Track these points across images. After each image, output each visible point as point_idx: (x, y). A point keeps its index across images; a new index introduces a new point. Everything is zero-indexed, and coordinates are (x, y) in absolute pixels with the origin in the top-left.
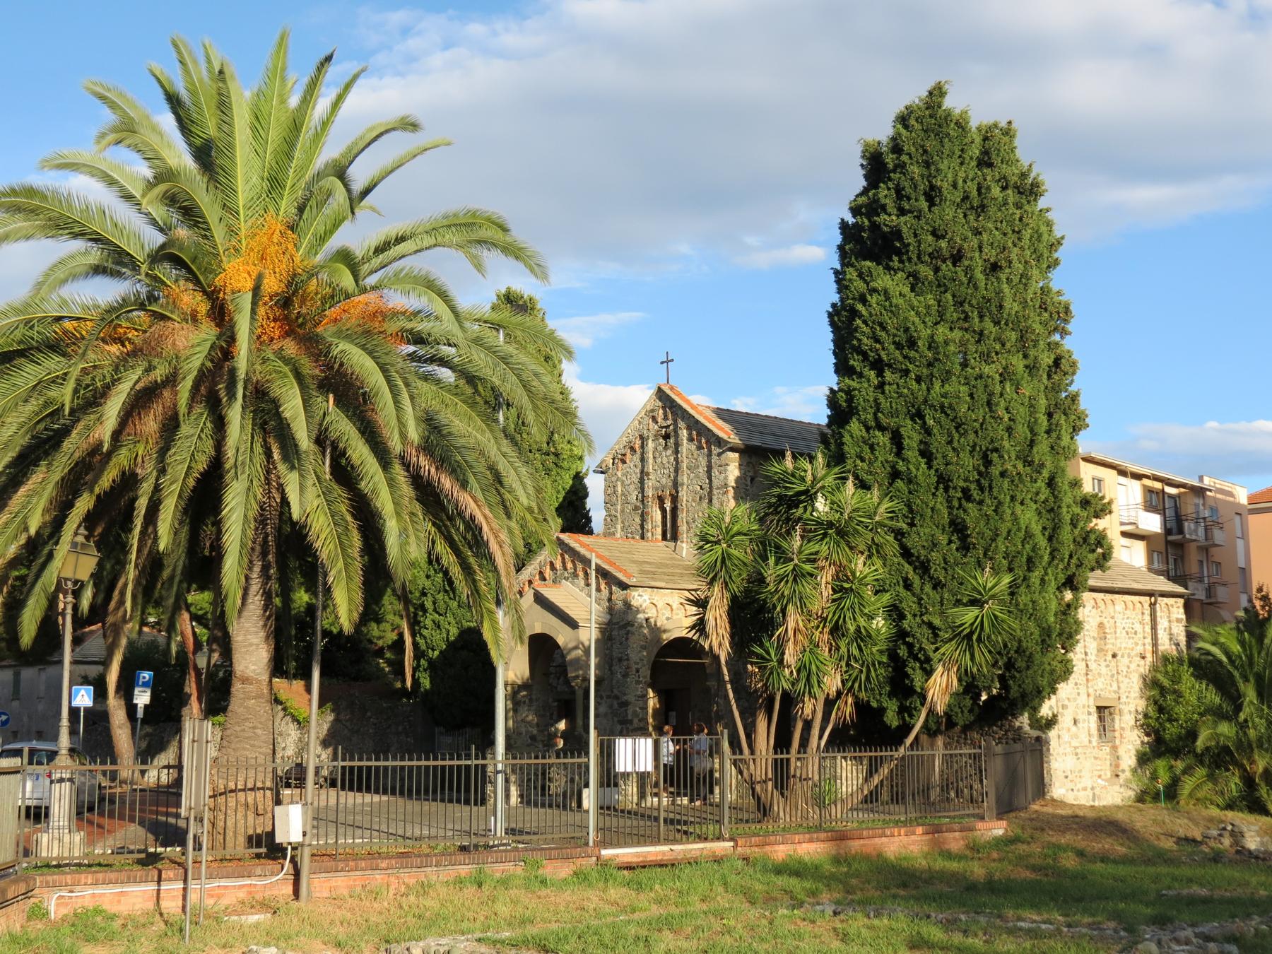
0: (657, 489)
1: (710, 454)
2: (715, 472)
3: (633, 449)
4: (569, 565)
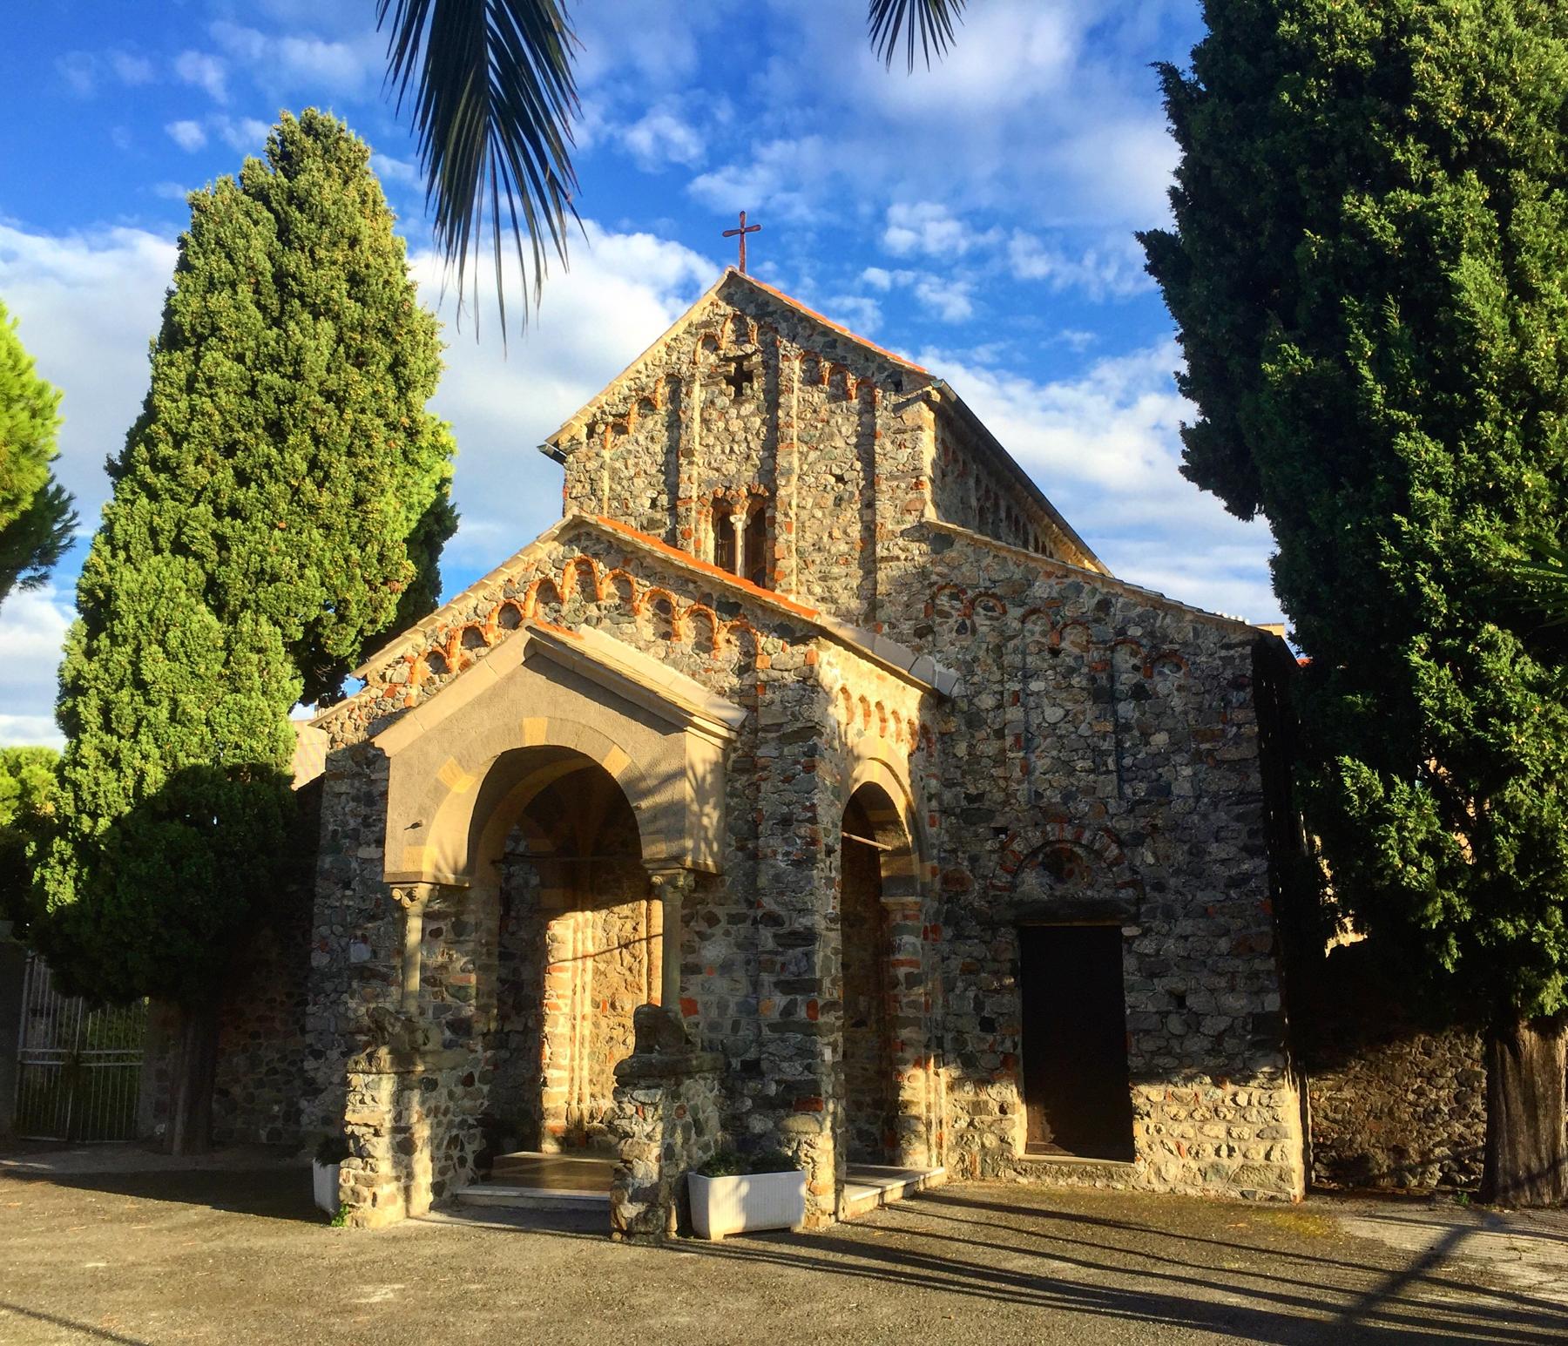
0: (710, 483)
1: (869, 406)
2: (883, 445)
3: (647, 404)
4: (607, 588)
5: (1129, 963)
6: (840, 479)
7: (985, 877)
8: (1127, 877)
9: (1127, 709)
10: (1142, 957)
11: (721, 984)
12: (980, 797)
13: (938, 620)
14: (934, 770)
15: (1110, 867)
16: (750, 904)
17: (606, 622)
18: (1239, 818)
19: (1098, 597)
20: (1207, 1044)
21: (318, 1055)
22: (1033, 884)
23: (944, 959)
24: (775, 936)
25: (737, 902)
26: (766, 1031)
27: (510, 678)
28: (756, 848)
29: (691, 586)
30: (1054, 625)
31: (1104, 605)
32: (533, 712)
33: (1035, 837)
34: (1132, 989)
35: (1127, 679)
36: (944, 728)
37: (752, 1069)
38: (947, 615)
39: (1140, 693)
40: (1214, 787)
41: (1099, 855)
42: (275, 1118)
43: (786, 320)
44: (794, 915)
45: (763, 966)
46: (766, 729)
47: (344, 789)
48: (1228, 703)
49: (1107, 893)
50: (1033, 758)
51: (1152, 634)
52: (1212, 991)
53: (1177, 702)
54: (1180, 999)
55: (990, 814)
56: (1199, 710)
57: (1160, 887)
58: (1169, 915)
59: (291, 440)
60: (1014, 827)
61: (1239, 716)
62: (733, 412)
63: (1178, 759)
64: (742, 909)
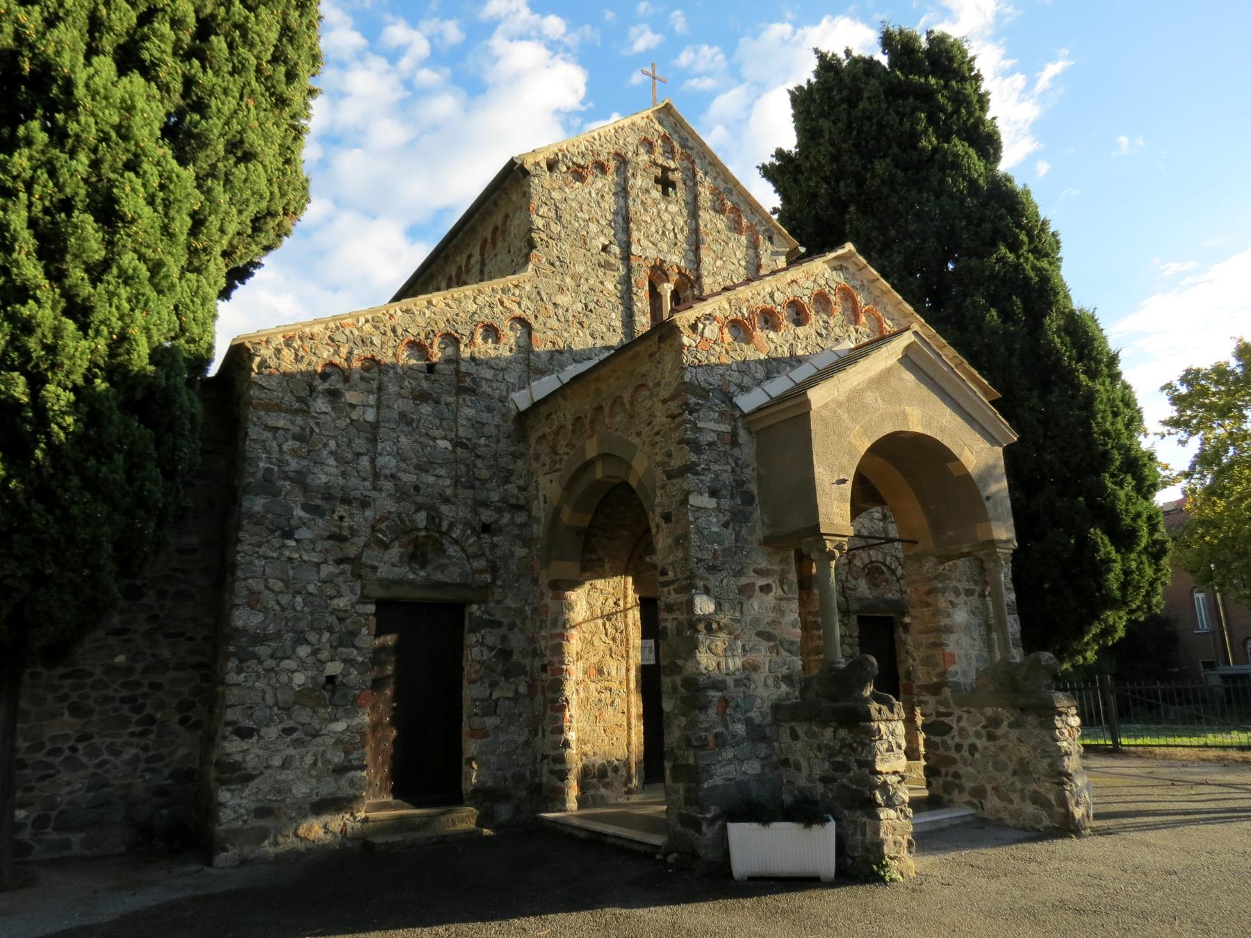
15: (898, 580)
16: (976, 583)
21: (244, 733)
27: (889, 371)
47: (281, 424)
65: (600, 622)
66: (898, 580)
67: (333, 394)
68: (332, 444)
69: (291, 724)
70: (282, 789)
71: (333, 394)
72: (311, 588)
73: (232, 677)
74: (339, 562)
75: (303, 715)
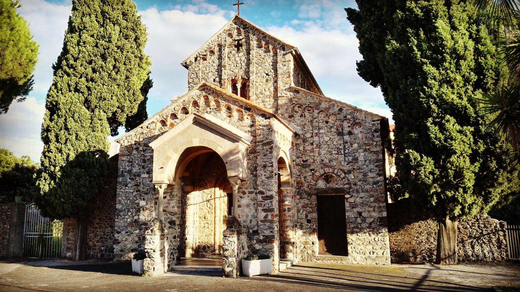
0: (230, 75)
1: (276, 54)
2: (279, 65)
3: (212, 52)
4: (213, 103)
5: (347, 204)
6: (267, 74)
7: (308, 182)
8: (347, 182)
9: (347, 138)
10: (350, 203)
11: (247, 210)
12: (306, 161)
13: (295, 113)
14: (294, 154)
15: (342, 179)
16: (255, 189)
17: (212, 113)
18: (376, 166)
19: (339, 107)
20: (367, 225)
21: (118, 233)
22: (321, 184)
23: (297, 204)
24: (262, 197)
25: (251, 188)
26: (260, 222)
27: (188, 128)
28: (256, 174)
29: (237, 103)
30: (327, 115)
31: (341, 110)
32: (195, 137)
33: (322, 172)
34: (348, 211)
35: (346, 130)
36: (297, 142)
37: (256, 232)
38: (297, 112)
39: (350, 133)
40: (370, 158)
41: (339, 176)
42: (102, 251)
43: (252, 29)
44: (267, 191)
45: (258, 205)
46: (259, 142)
48: (374, 136)
49: (341, 186)
50: (321, 150)
51: (353, 118)
52: (369, 212)
53: (360, 136)
54: (360, 214)
55: (310, 165)
56: (366, 138)
57: (355, 184)
58: (358, 192)
59: (108, 60)
60: (316, 169)
61: (377, 139)
62: (237, 55)
63: (360, 151)
64: (252, 190)
65: (206, 203)
66: (342, 179)
67: (137, 149)
68: (137, 162)
69: (127, 231)
70: (125, 246)
71: (137, 149)
72: (131, 198)
73: (116, 220)
74: (137, 191)
75: (129, 229)
